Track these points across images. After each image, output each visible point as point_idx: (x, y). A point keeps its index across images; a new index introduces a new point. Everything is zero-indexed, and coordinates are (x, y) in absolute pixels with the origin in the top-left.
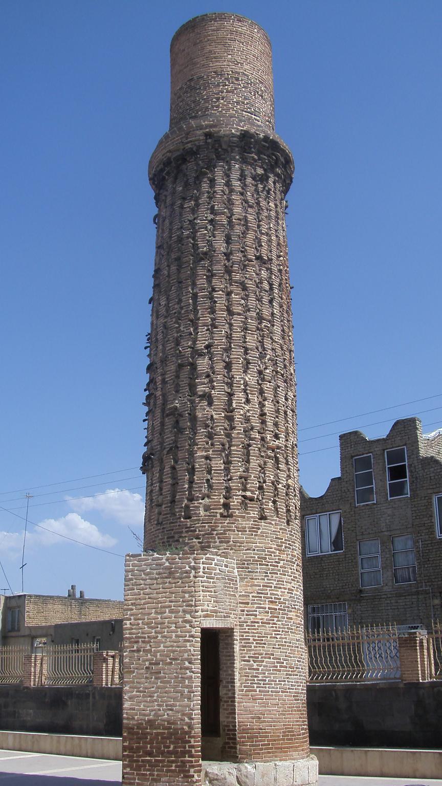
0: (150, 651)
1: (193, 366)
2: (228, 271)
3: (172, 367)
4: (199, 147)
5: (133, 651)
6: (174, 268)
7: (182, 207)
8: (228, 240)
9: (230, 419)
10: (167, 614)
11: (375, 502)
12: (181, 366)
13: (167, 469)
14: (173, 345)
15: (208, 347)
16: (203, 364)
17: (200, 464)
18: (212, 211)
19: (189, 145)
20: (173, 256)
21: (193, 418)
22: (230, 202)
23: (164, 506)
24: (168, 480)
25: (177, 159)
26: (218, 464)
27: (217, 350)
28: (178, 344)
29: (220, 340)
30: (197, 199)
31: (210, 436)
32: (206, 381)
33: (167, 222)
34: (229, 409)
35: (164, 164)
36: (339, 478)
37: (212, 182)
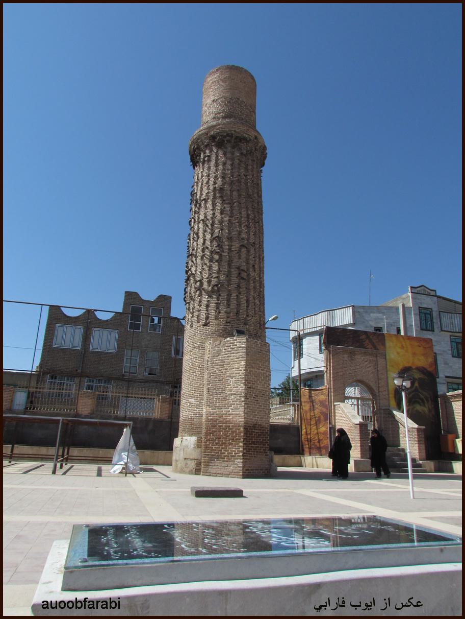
0: (254, 388)
3: (236, 245)
4: (250, 140)
5: (249, 388)
6: (235, 194)
10: (261, 371)
11: (140, 331)
13: (234, 295)
14: (237, 233)
15: (254, 243)
17: (251, 299)
19: (246, 136)
21: (248, 275)
23: (231, 314)
25: (237, 137)
28: (240, 234)
32: (253, 259)
35: (227, 134)
36: (121, 313)
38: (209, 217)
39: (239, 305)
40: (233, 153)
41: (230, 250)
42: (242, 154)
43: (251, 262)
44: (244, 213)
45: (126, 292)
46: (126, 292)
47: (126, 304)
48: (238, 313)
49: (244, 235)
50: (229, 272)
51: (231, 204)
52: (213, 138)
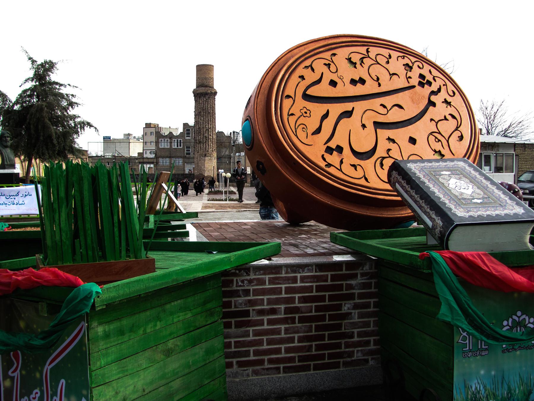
1: (209, 130)
2: (212, 116)
3: (205, 130)
6: (204, 113)
7: (206, 103)
8: (212, 110)
9: (213, 138)
12: (206, 130)
16: (210, 130)
17: (209, 144)
18: (210, 105)
20: (205, 111)
21: (209, 138)
22: (212, 104)
24: (205, 146)
26: (212, 145)
27: (211, 128)
29: (212, 127)
30: (208, 102)
31: (211, 140)
33: (202, 104)
34: (213, 137)
37: (210, 100)
38: (198, 121)
39: (206, 147)
40: (204, 99)
41: (203, 131)
42: (206, 99)
43: (210, 134)
44: (207, 119)
45: (183, 124)
46: (183, 124)
47: (184, 128)
48: (206, 149)
49: (207, 126)
50: (203, 137)
51: (203, 117)
52: (198, 94)
